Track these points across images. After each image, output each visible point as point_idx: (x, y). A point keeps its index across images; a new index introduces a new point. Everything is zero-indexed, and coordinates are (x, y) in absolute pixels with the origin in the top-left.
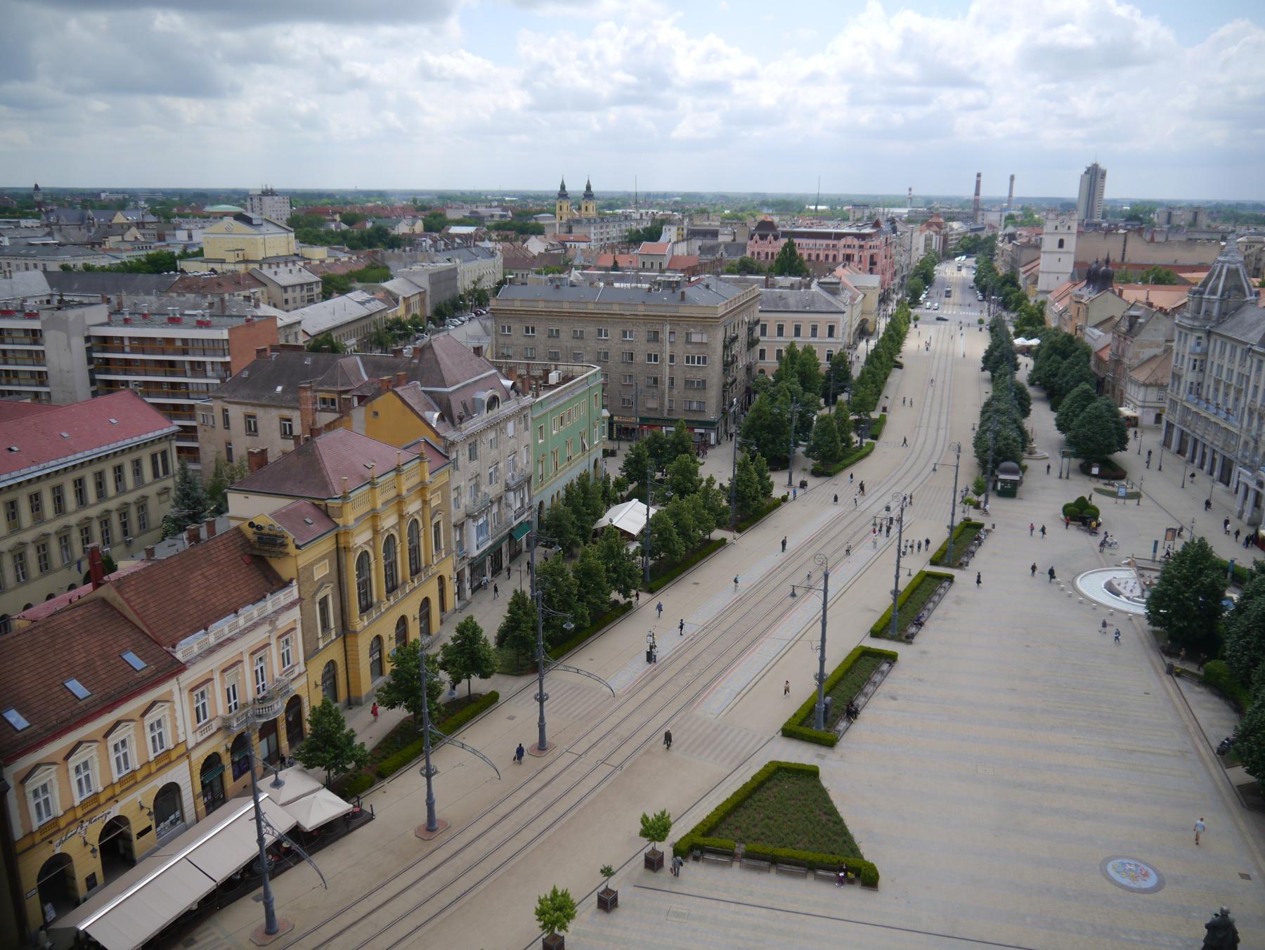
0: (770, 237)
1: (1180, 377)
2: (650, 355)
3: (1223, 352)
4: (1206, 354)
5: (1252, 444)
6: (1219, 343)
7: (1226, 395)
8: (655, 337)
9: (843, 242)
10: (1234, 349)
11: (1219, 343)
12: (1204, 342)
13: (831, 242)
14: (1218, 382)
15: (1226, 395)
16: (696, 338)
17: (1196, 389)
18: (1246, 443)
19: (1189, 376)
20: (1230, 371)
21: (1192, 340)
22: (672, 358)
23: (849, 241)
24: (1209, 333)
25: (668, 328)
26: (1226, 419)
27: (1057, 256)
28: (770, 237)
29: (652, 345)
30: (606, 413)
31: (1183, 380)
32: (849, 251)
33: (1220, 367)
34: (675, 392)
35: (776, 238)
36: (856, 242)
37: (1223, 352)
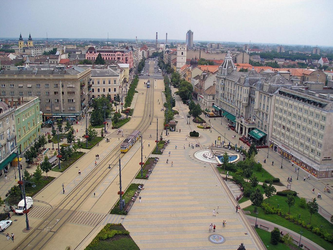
0: (93, 52)
1: (218, 92)
2: (55, 92)
3: (229, 84)
4: (225, 85)
5: (238, 111)
6: (228, 82)
7: (231, 97)
8: (57, 86)
9: (117, 53)
10: (232, 83)
11: (228, 82)
12: (224, 82)
13: (113, 54)
14: (228, 93)
15: (231, 97)
16: (71, 86)
17: (223, 96)
18: (237, 110)
19: (221, 92)
20: (231, 90)
21: (220, 81)
22: (63, 93)
23: (119, 53)
24: (225, 79)
25: (61, 83)
26: (231, 104)
27: (181, 57)
28: (93, 52)
29: (56, 89)
30: (41, 112)
31: (219, 93)
32: (119, 56)
33: (229, 89)
34: (65, 104)
35: (95, 53)
36: (121, 54)
37: (229, 84)
